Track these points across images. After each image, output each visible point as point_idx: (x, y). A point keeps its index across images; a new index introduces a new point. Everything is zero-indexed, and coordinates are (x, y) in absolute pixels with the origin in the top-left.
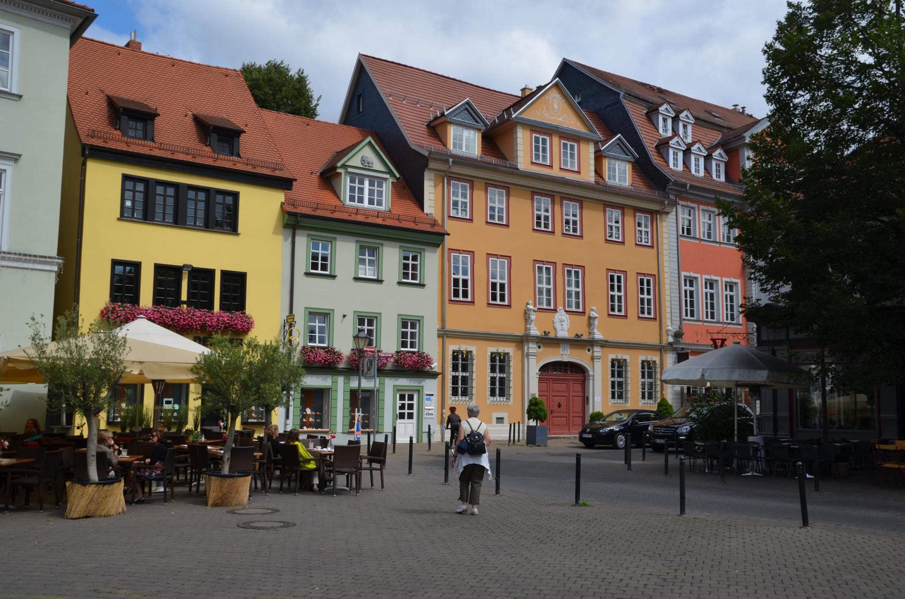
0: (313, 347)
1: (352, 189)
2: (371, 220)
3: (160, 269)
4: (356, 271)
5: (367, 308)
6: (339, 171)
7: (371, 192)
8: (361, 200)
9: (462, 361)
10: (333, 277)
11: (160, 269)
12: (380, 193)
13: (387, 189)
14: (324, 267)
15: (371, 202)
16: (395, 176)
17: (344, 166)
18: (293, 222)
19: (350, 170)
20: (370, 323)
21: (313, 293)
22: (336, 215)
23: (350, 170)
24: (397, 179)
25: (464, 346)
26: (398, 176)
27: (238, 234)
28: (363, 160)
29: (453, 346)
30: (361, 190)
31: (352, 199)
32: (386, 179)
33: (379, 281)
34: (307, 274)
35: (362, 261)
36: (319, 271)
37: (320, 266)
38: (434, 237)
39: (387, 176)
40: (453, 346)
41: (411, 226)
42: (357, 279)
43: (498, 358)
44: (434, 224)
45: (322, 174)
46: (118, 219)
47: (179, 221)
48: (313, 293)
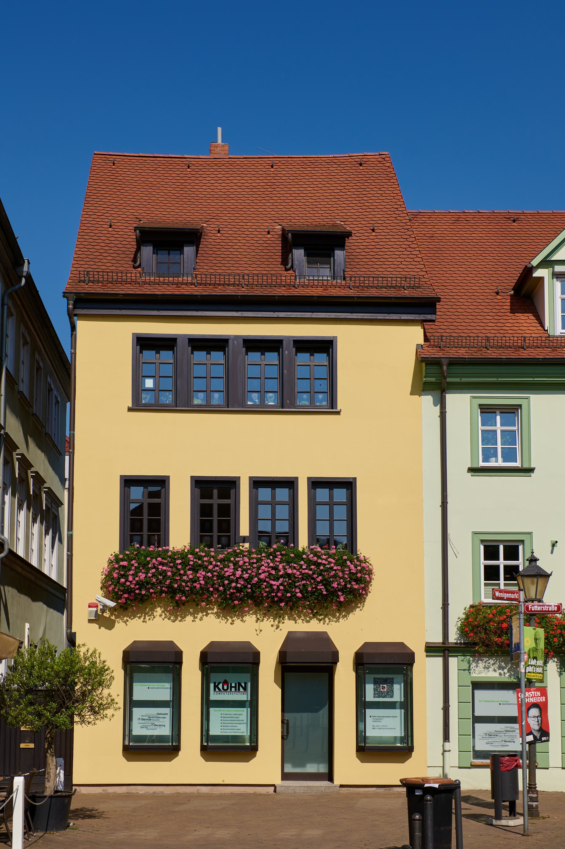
3: (203, 486)
6: (538, 273)
11: (203, 486)
17: (546, 263)
18: (436, 375)
19: (559, 269)
22: (524, 354)
23: (559, 269)
46: (130, 410)
47: (234, 402)
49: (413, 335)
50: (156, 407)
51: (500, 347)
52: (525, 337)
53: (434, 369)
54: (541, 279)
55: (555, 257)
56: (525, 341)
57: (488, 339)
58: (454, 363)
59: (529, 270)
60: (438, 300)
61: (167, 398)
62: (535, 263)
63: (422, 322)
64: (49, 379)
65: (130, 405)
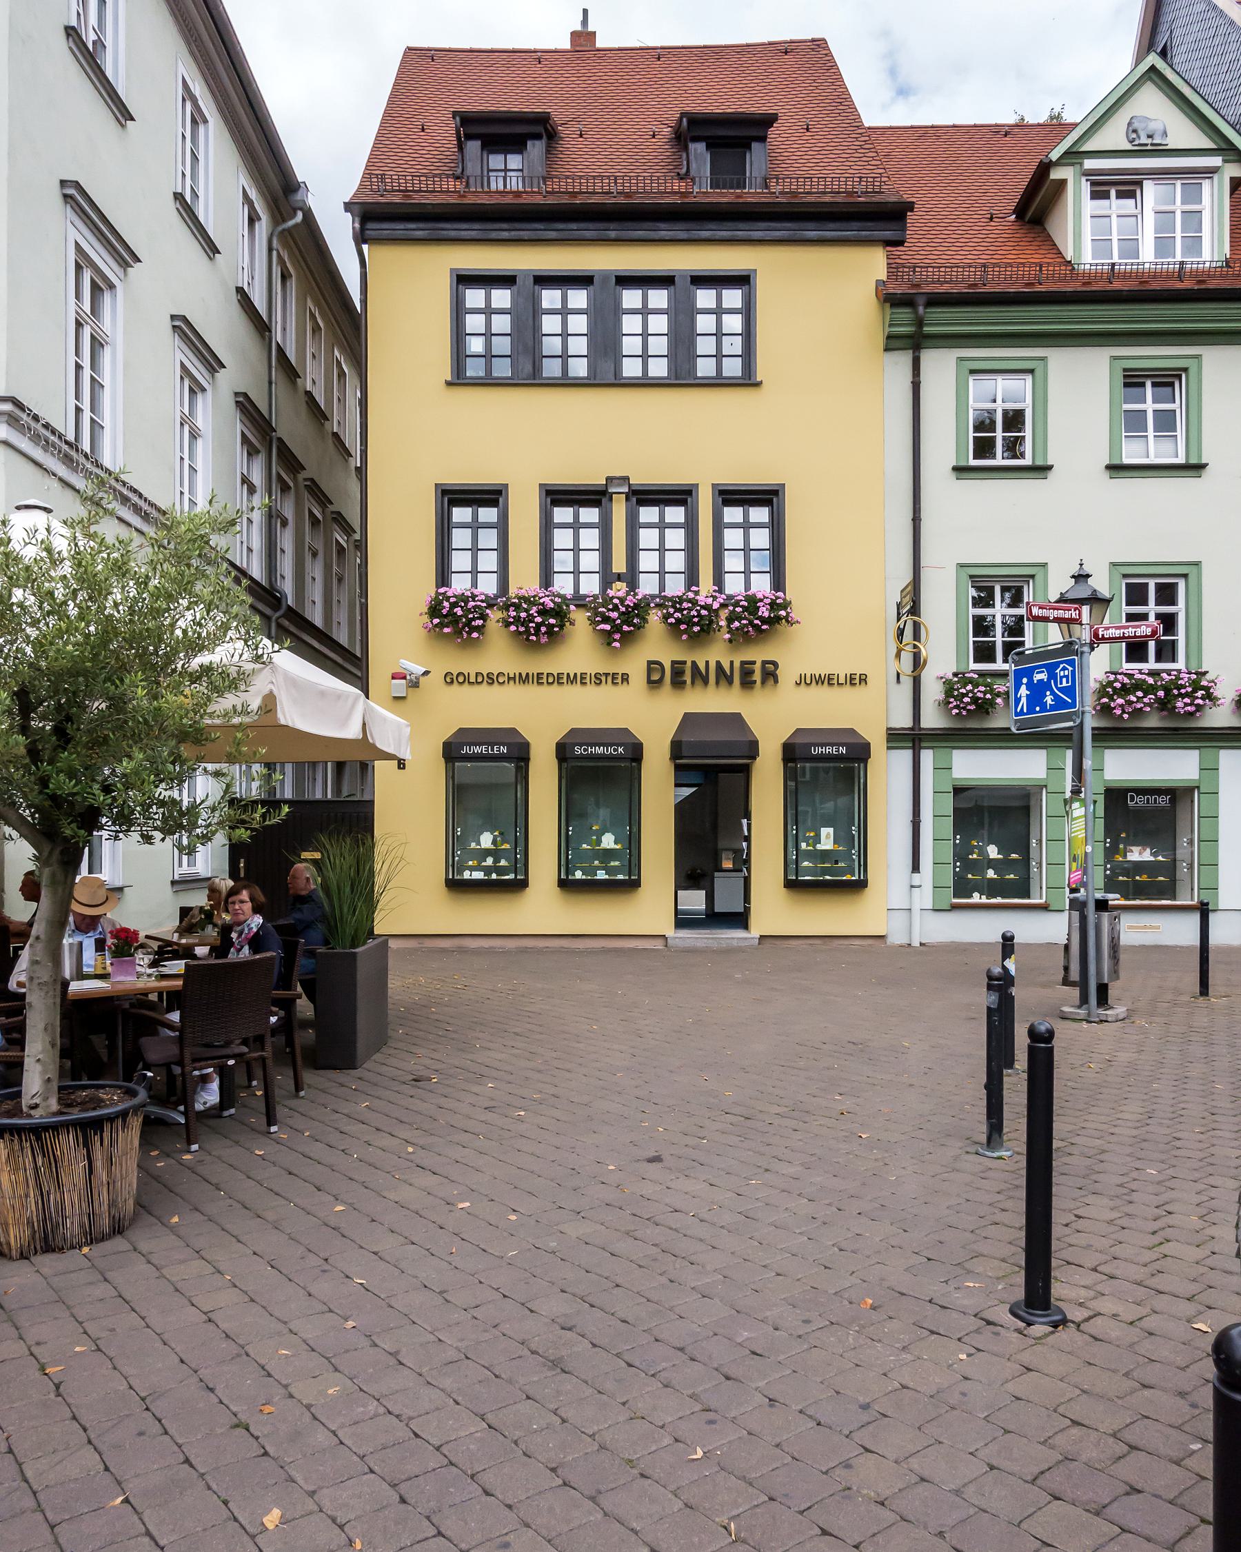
0: (982, 674)
2: (1155, 286)
4: (1114, 446)
6: (1056, 174)
10: (1041, 470)
14: (1013, 447)
19: (1089, 164)
20: (1167, 594)
21: (983, 524)
23: (1089, 164)
27: (758, 385)
28: (1132, 130)
32: (1211, 171)
33: (1195, 468)
35: (1135, 422)
36: (999, 461)
37: (999, 446)
39: (1216, 161)
42: (1116, 469)
45: (1021, 211)
46: (449, 384)
48: (983, 524)
49: (871, 265)
50: (488, 382)
53: (905, 314)
54: (1063, 183)
55: (1089, 146)
59: (1044, 168)
60: (910, 206)
61: (502, 369)
62: (1054, 156)
63: (888, 243)
64: (337, 353)
65: (449, 379)
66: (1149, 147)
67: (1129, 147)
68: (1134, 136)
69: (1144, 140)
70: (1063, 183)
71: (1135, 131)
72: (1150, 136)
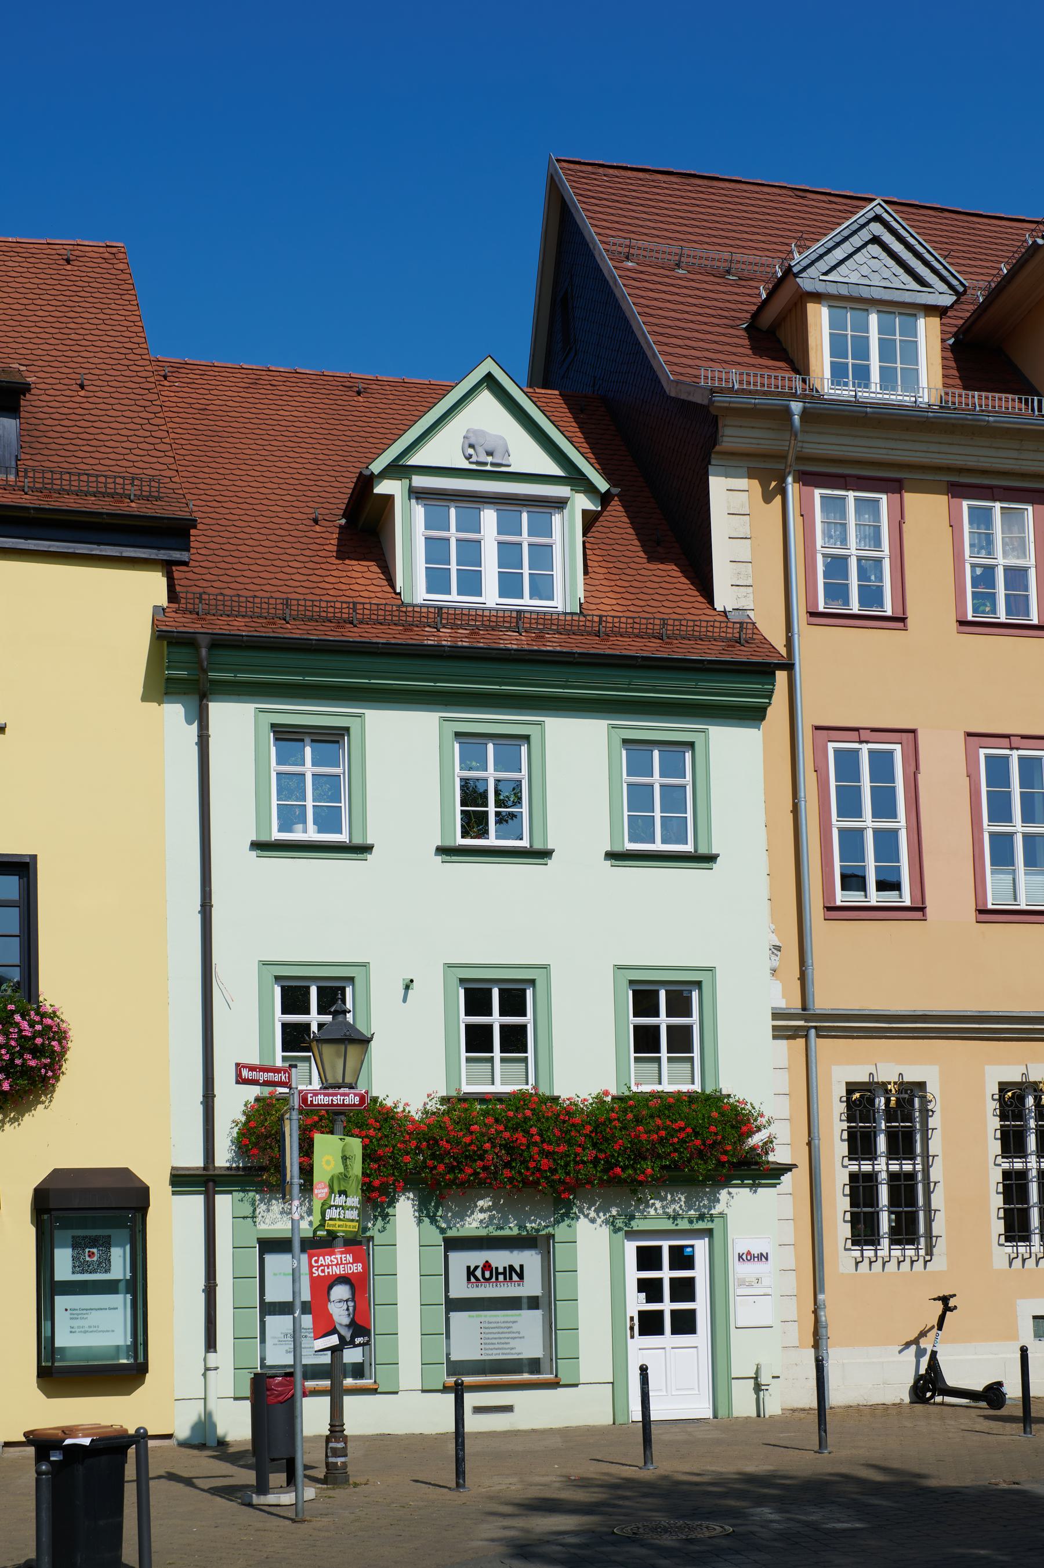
1: (436, 549)
5: (497, 952)
6: (384, 487)
7: (508, 553)
8: (471, 583)
9: (886, 1120)
12: (542, 555)
13: (565, 532)
15: (509, 585)
16: (590, 489)
17: (397, 469)
18: (190, 666)
19: (420, 481)
22: (353, 634)
23: (420, 481)
24: (605, 499)
25: (889, 1063)
26: (603, 486)
29: (847, 1064)
30: (471, 551)
31: (437, 581)
34: (261, 846)
38: (739, 678)
40: (847, 1064)
41: (651, 649)
43: (1030, 1101)
44: (744, 631)
51: (311, 619)
52: (355, 604)
53: (183, 654)
54: (389, 499)
55: (415, 460)
56: (355, 609)
57: (287, 602)
58: (221, 643)
59: (367, 481)
62: (376, 467)
66: (489, 468)
67: (465, 465)
68: (471, 451)
69: (484, 458)
70: (389, 499)
71: (472, 446)
72: (490, 453)
